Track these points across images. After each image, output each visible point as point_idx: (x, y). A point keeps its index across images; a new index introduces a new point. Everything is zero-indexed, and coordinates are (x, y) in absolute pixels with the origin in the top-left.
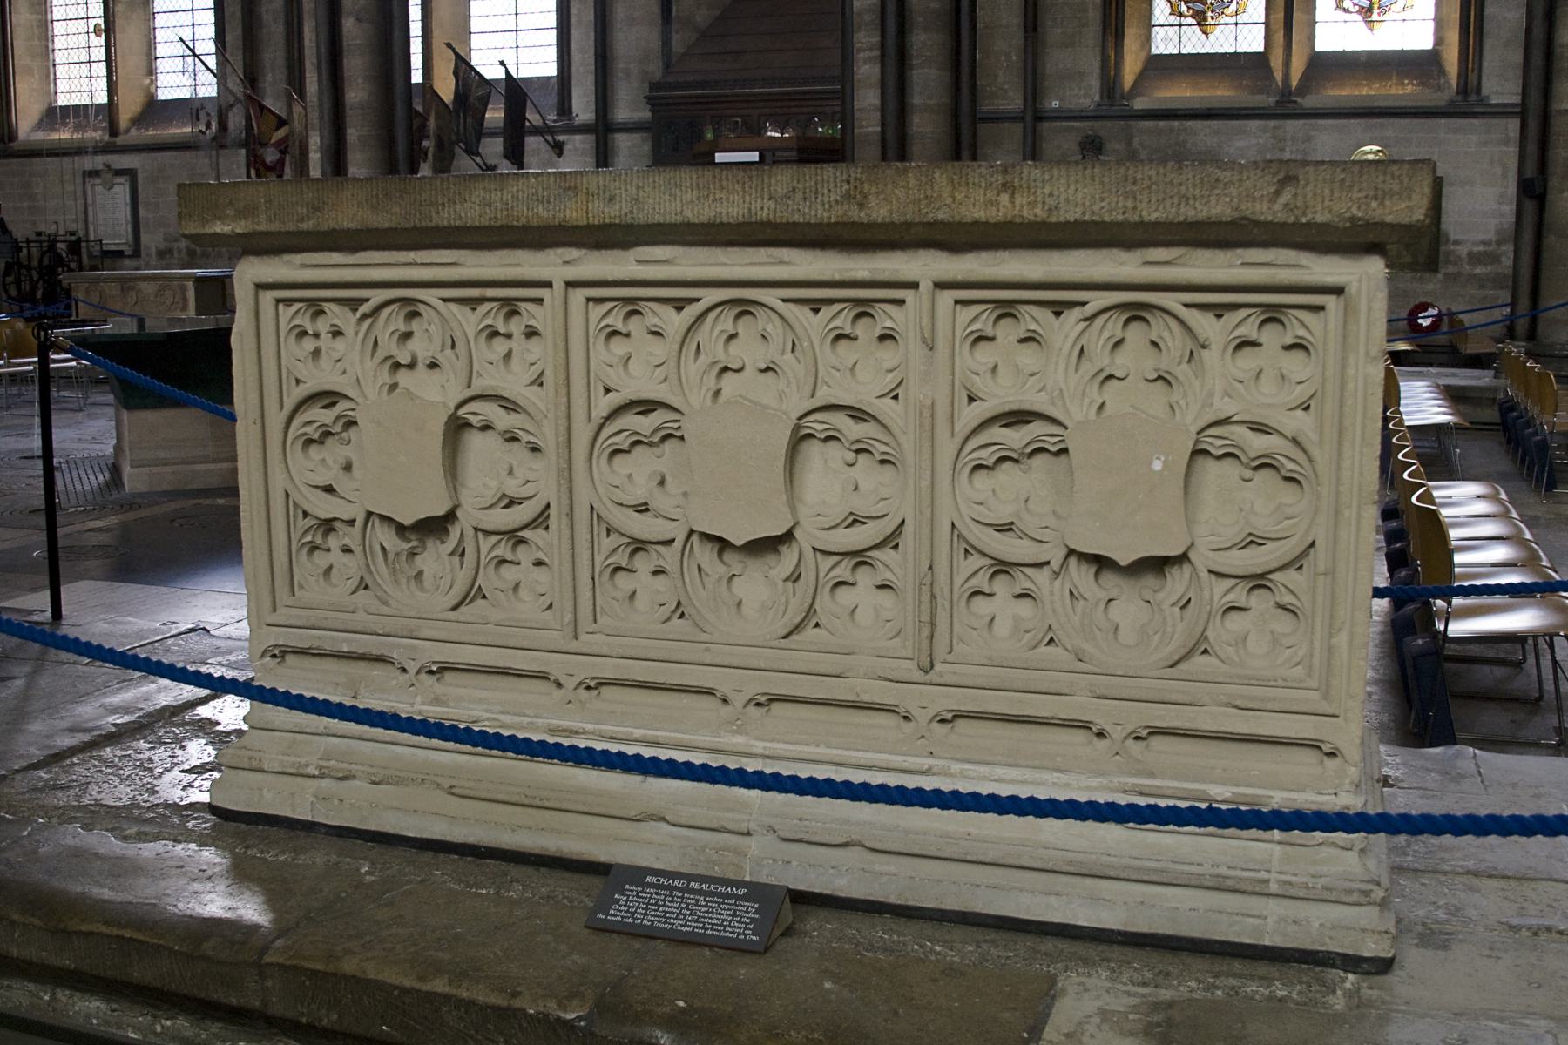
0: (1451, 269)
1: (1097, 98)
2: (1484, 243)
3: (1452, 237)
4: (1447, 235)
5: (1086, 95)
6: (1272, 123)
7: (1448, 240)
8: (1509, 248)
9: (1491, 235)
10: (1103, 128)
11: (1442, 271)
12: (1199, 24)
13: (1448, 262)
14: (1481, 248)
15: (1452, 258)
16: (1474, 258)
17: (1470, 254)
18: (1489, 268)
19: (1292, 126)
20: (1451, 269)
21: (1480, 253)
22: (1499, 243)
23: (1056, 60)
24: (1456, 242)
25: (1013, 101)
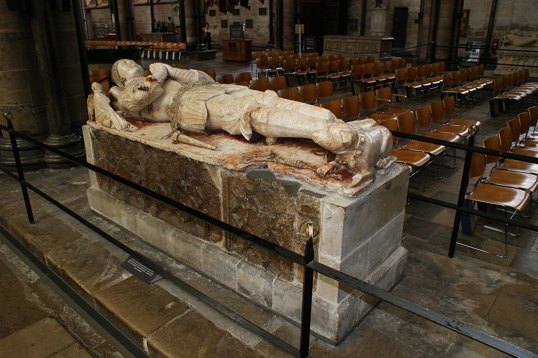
0: (470, 37)
2: (480, 29)
3: (471, 27)
4: (470, 27)
7: (470, 28)
8: (486, 31)
9: (482, 27)
11: (468, 37)
13: (469, 35)
14: (479, 31)
15: (470, 33)
16: (477, 34)
17: (476, 32)
18: (481, 36)
20: (470, 37)
21: (478, 32)
22: (484, 29)
24: (472, 29)
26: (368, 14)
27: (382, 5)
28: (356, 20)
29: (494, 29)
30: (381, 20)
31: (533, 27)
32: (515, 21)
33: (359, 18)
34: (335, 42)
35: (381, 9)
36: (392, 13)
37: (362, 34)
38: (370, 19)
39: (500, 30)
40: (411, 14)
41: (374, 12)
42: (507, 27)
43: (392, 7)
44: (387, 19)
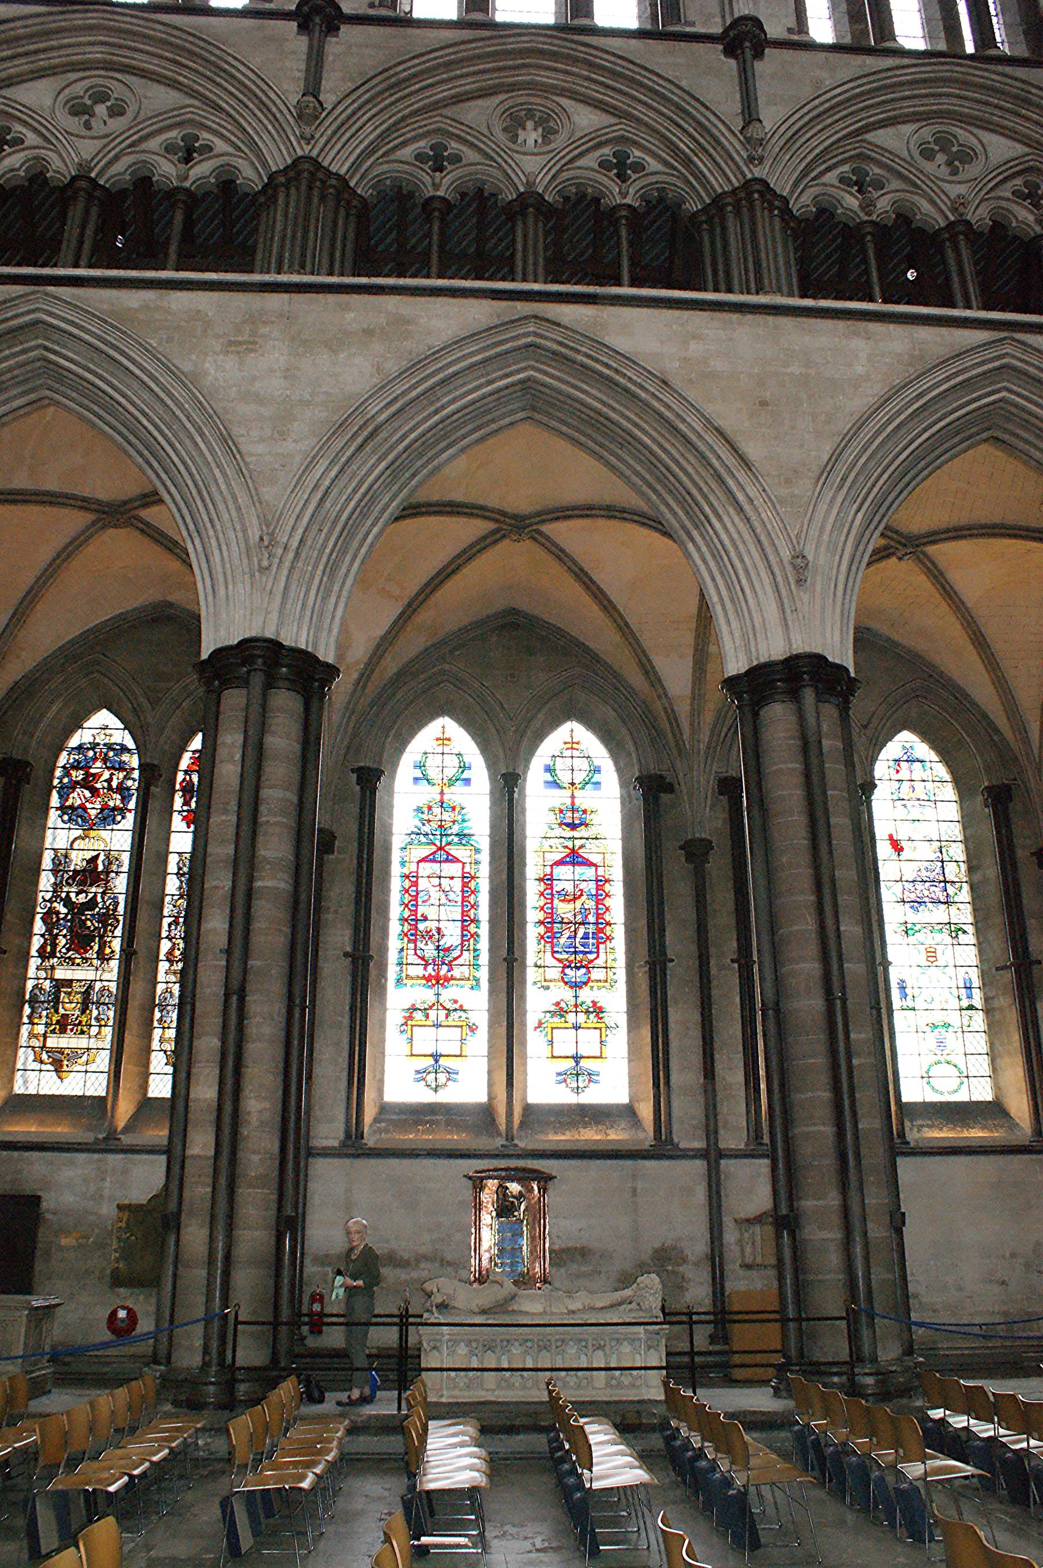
6: (96, 1156)
12: (56, 1070)
19: (114, 1160)
31: (406, 1256)
39: (323, 1264)
40: (49, 1216)
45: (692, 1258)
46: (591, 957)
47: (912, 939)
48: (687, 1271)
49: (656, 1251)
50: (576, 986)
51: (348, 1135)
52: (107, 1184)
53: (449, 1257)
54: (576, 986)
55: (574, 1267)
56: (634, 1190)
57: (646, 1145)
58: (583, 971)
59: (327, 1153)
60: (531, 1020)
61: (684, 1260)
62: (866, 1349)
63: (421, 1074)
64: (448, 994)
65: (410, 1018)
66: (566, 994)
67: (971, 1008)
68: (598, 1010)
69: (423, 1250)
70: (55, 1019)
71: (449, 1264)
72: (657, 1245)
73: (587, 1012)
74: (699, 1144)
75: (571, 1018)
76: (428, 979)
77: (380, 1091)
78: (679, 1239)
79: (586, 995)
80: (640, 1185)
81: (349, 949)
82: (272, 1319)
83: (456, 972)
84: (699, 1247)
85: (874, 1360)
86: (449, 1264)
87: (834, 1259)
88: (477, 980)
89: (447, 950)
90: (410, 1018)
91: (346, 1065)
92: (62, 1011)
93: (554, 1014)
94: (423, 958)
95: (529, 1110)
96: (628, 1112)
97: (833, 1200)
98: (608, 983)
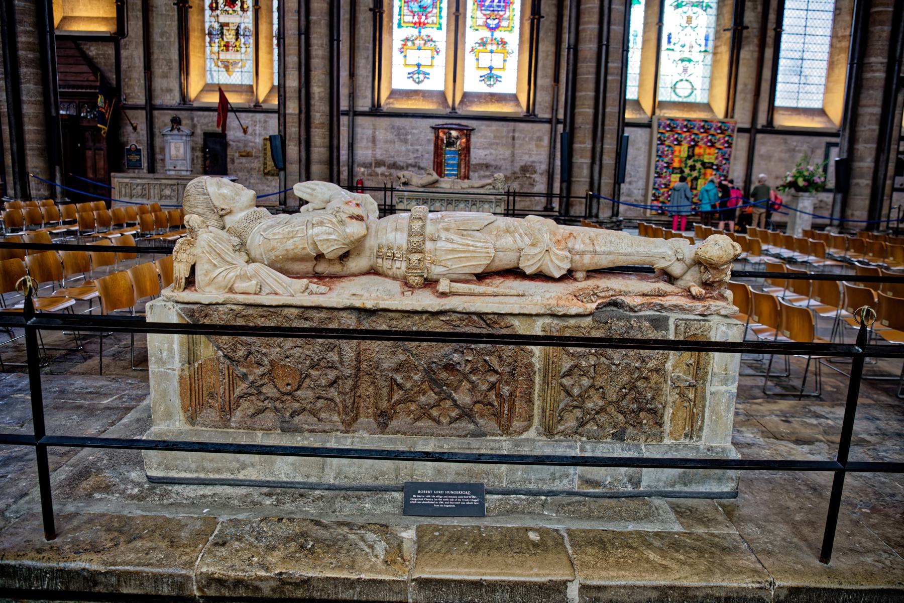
1: (178, 101)
5: (173, 99)
6: (251, 114)
10: (183, 115)
23: (159, 83)
25: (142, 101)
26: (158, 141)
27: (182, 127)
28: (138, 151)
29: (355, 166)
30: (182, 151)
31: (402, 164)
32: (379, 157)
33: (143, 147)
34: (138, 185)
35: (181, 133)
36: (200, 140)
37: (152, 169)
38: (163, 149)
40: (231, 143)
41: (169, 138)
42: (371, 164)
43: (199, 131)
44: (193, 149)
45: (539, 171)
46: (501, 13)
47: (680, 10)
48: (536, 177)
49: (522, 167)
50: (492, 29)
51: (373, 105)
52: (257, 128)
53: (422, 165)
54: (492, 29)
55: (482, 173)
56: (513, 138)
57: (522, 115)
58: (497, 21)
59: (364, 114)
60: (468, 48)
61: (535, 172)
62: (594, 211)
63: (411, 75)
64: (425, 32)
65: (405, 45)
66: (486, 33)
67: (706, 51)
68: (503, 43)
69: (410, 162)
70: (223, 43)
71: (422, 169)
72: (523, 164)
73: (498, 44)
74: (547, 116)
75: (489, 47)
76: (415, 24)
77: (390, 83)
78: (533, 162)
79: (498, 34)
80: (517, 135)
81: (372, 6)
82: (156, 113)
83: (430, 20)
84: (544, 167)
85: (597, 216)
86: (422, 169)
87: (586, 172)
88: (440, 24)
89: (425, 8)
90: (405, 45)
91: (371, 69)
92: (225, 40)
93: (480, 45)
94: (412, 12)
95: (465, 95)
96: (514, 98)
97: (588, 145)
98: (510, 29)
